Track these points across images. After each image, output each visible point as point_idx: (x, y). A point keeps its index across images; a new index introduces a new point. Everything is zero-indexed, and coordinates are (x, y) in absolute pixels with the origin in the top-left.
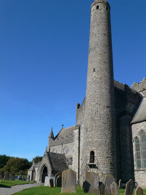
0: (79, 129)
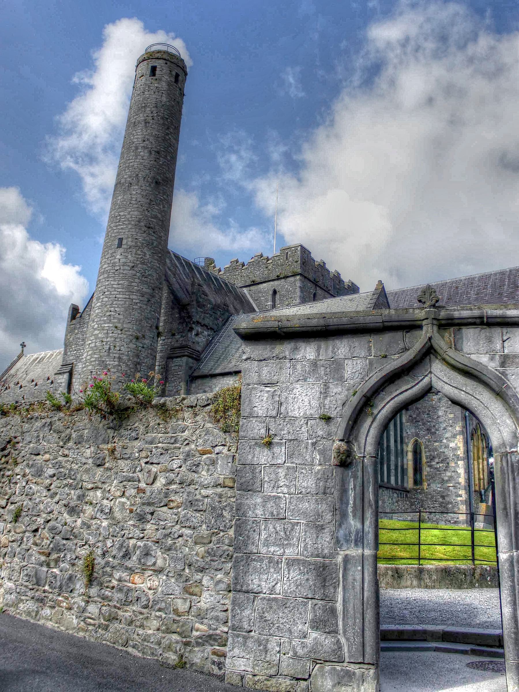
0: (71, 374)
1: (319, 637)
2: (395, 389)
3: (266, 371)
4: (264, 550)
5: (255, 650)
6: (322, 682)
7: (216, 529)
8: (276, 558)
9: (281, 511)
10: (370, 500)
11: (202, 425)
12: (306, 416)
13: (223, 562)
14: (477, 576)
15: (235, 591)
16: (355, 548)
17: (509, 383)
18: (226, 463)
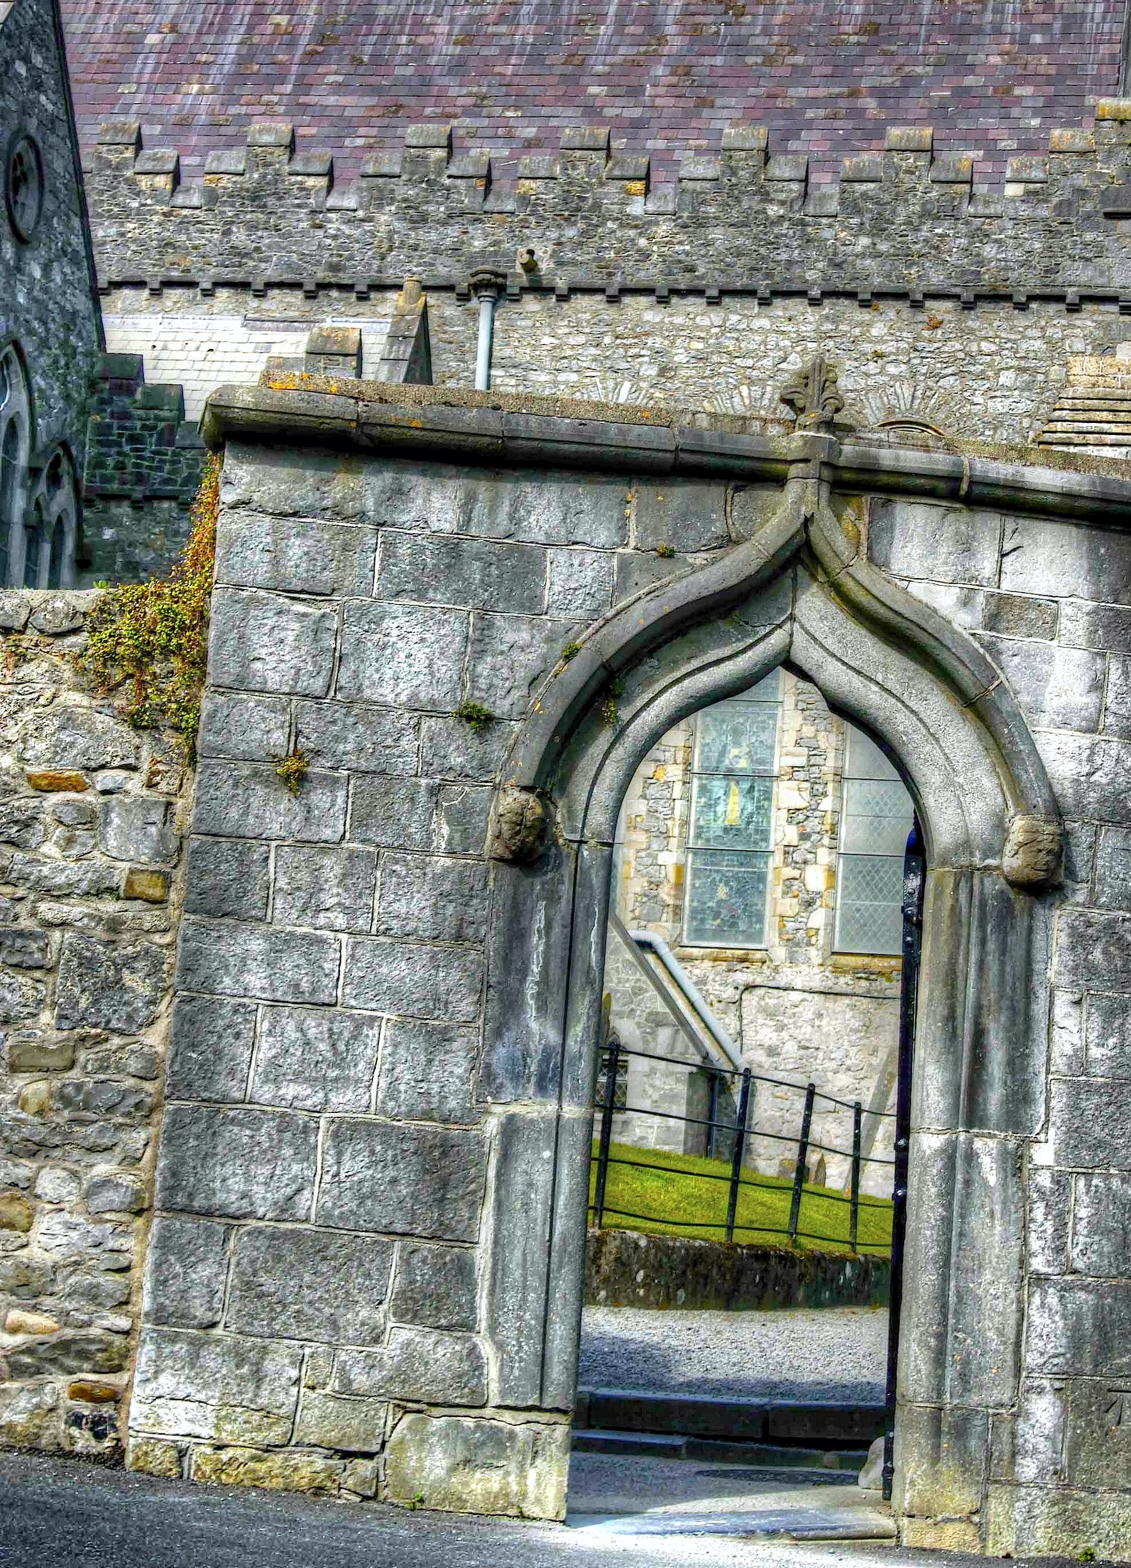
1: (417, 1339)
2: (687, 652)
3: (300, 552)
4: (266, 1093)
5: (224, 1377)
6: (420, 1459)
7: (95, 1026)
8: (302, 1117)
9: (325, 981)
10: (590, 967)
11: (48, 694)
12: (417, 706)
13: (119, 1127)
14: (606, 1264)
15: (168, 1210)
16: (539, 1099)
17: (1002, 676)
18: (139, 823)
